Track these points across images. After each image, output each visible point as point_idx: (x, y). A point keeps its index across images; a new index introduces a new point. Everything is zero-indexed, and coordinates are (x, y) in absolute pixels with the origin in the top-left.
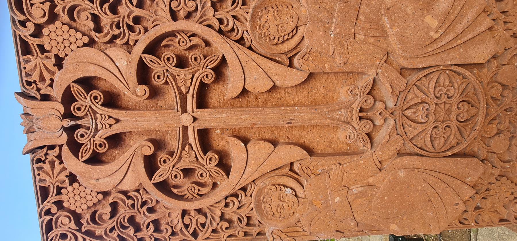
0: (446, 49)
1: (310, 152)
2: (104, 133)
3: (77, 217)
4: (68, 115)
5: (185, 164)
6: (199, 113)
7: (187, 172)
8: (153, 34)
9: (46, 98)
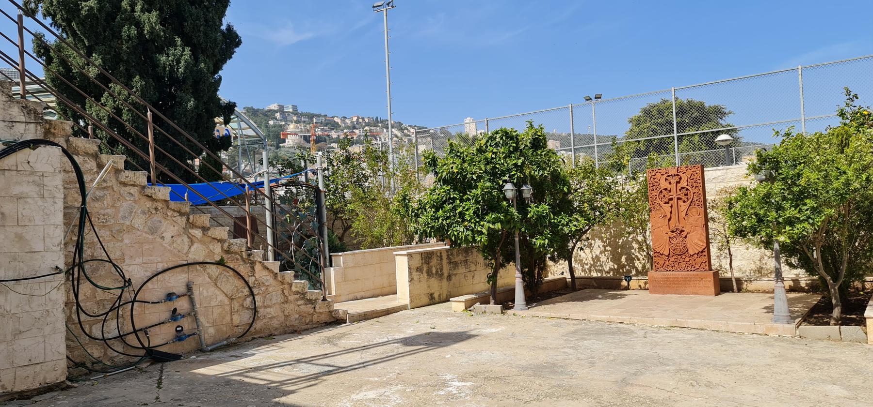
0: (691, 244)
1: (670, 220)
2: (671, 181)
3: (654, 175)
4: (675, 175)
5: (666, 196)
6: (676, 199)
7: (664, 196)
8: (690, 189)
9: (678, 170)
